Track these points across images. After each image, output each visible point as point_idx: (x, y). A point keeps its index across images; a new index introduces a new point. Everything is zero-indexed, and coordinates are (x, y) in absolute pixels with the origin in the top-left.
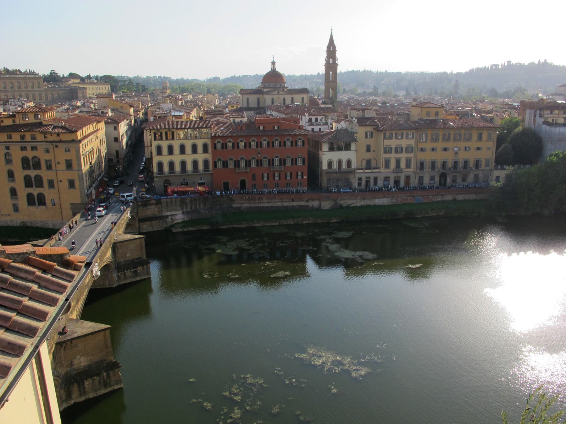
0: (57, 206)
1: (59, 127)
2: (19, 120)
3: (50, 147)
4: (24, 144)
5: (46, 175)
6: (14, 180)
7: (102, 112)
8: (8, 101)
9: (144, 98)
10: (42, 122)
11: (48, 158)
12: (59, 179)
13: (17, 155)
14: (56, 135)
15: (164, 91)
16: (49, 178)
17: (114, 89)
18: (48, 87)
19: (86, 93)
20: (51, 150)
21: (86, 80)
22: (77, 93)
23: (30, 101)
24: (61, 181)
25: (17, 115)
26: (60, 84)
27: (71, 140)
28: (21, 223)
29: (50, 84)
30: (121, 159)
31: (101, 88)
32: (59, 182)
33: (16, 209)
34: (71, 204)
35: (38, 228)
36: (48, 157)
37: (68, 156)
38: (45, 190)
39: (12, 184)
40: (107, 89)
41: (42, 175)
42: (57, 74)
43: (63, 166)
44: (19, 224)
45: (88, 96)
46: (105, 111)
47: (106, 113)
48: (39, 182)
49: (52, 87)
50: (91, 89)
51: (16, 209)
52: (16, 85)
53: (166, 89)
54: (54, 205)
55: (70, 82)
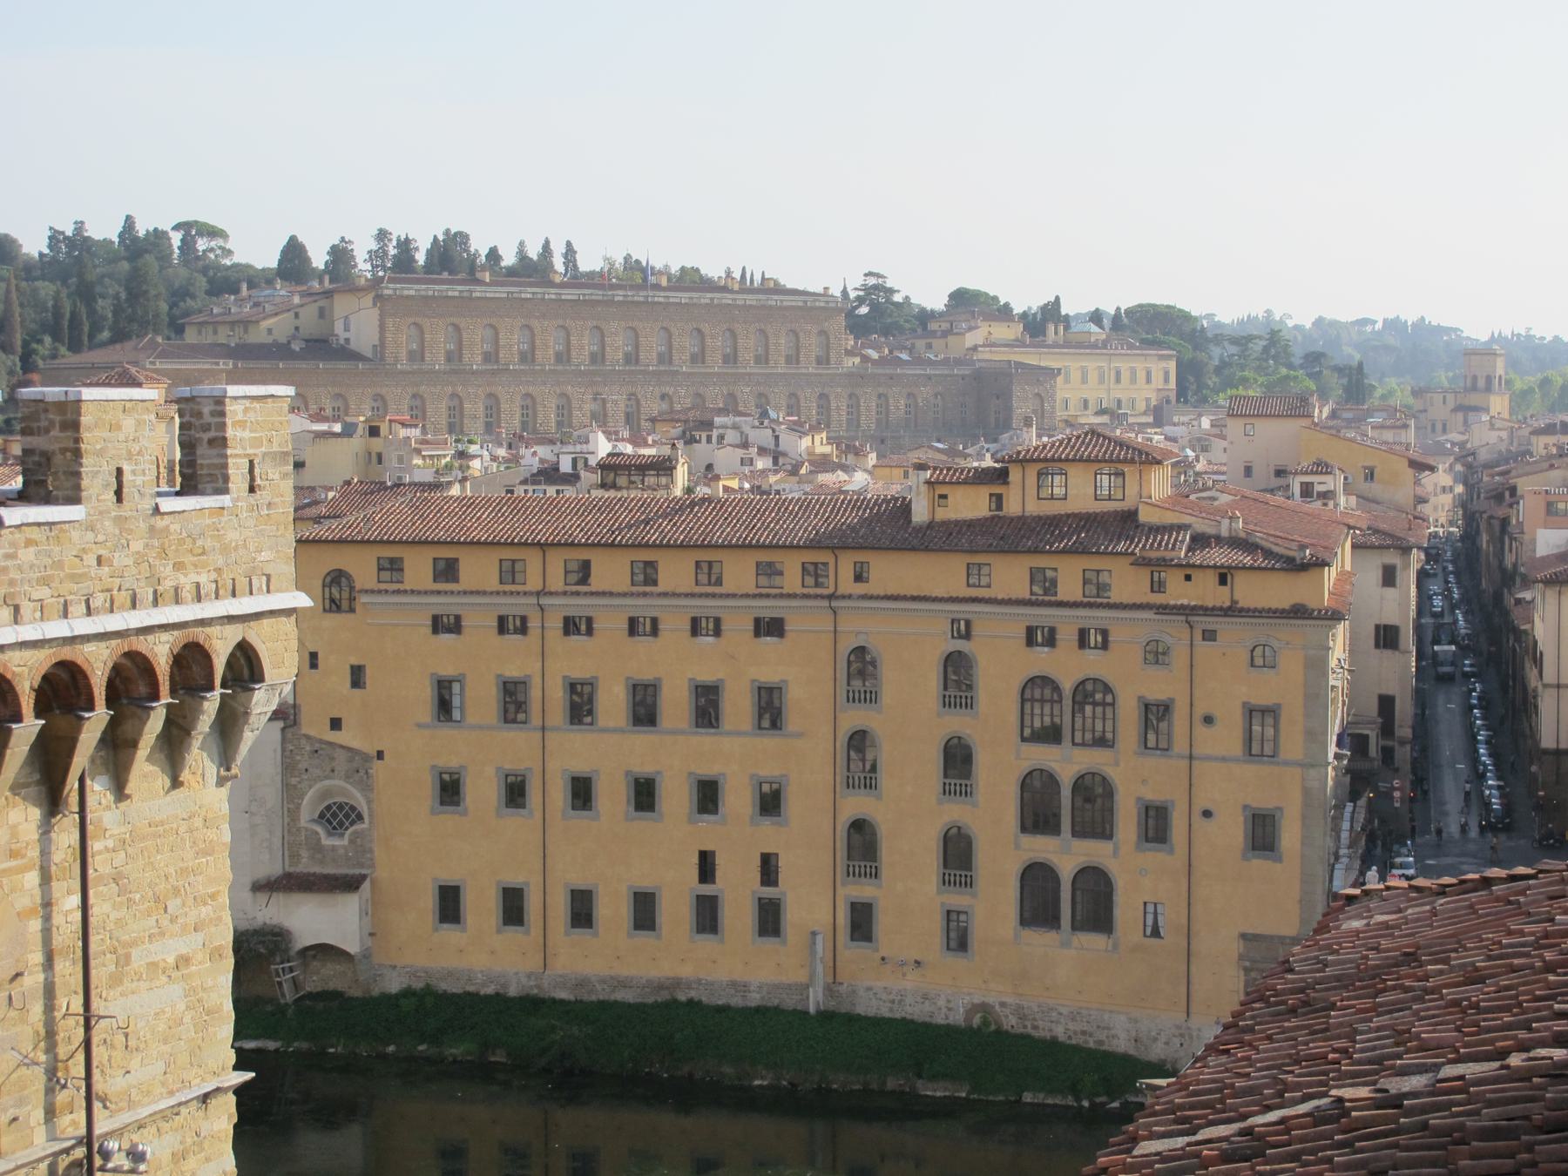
0: (1172, 938)
1: (1219, 539)
2: (1021, 500)
3: (1174, 633)
4: (1043, 616)
5: (1134, 778)
6: (967, 793)
7: (1307, 491)
8: (708, 425)
9: (1388, 436)
10: (1130, 517)
11: (1157, 694)
12: (1200, 804)
13: (1002, 664)
14: (1211, 578)
15: (1474, 399)
16: (1150, 795)
17: (1192, 385)
18: (865, 359)
19: (1053, 397)
20: (1179, 657)
21: (1051, 328)
22: (1005, 396)
23: (815, 429)
24: (1207, 814)
25: (1015, 475)
26: (920, 344)
27: (1286, 605)
28: (974, 1009)
29: (877, 348)
30: (1402, 743)
31: (1125, 376)
32: (1197, 818)
33: (958, 938)
34: (1244, 936)
35: (1053, 1044)
36: (1158, 685)
37: (1263, 690)
38: (1122, 857)
39: (955, 812)
40: (1158, 381)
41: (1115, 775)
42: (891, 291)
43: (1226, 738)
44: (958, 1018)
45: (1060, 414)
46: (1322, 483)
47: (1326, 496)
48: (1093, 807)
49: (882, 361)
50: (1075, 376)
51: (958, 938)
52: (717, 344)
53: (1488, 389)
54: (1156, 933)
55: (971, 339)
